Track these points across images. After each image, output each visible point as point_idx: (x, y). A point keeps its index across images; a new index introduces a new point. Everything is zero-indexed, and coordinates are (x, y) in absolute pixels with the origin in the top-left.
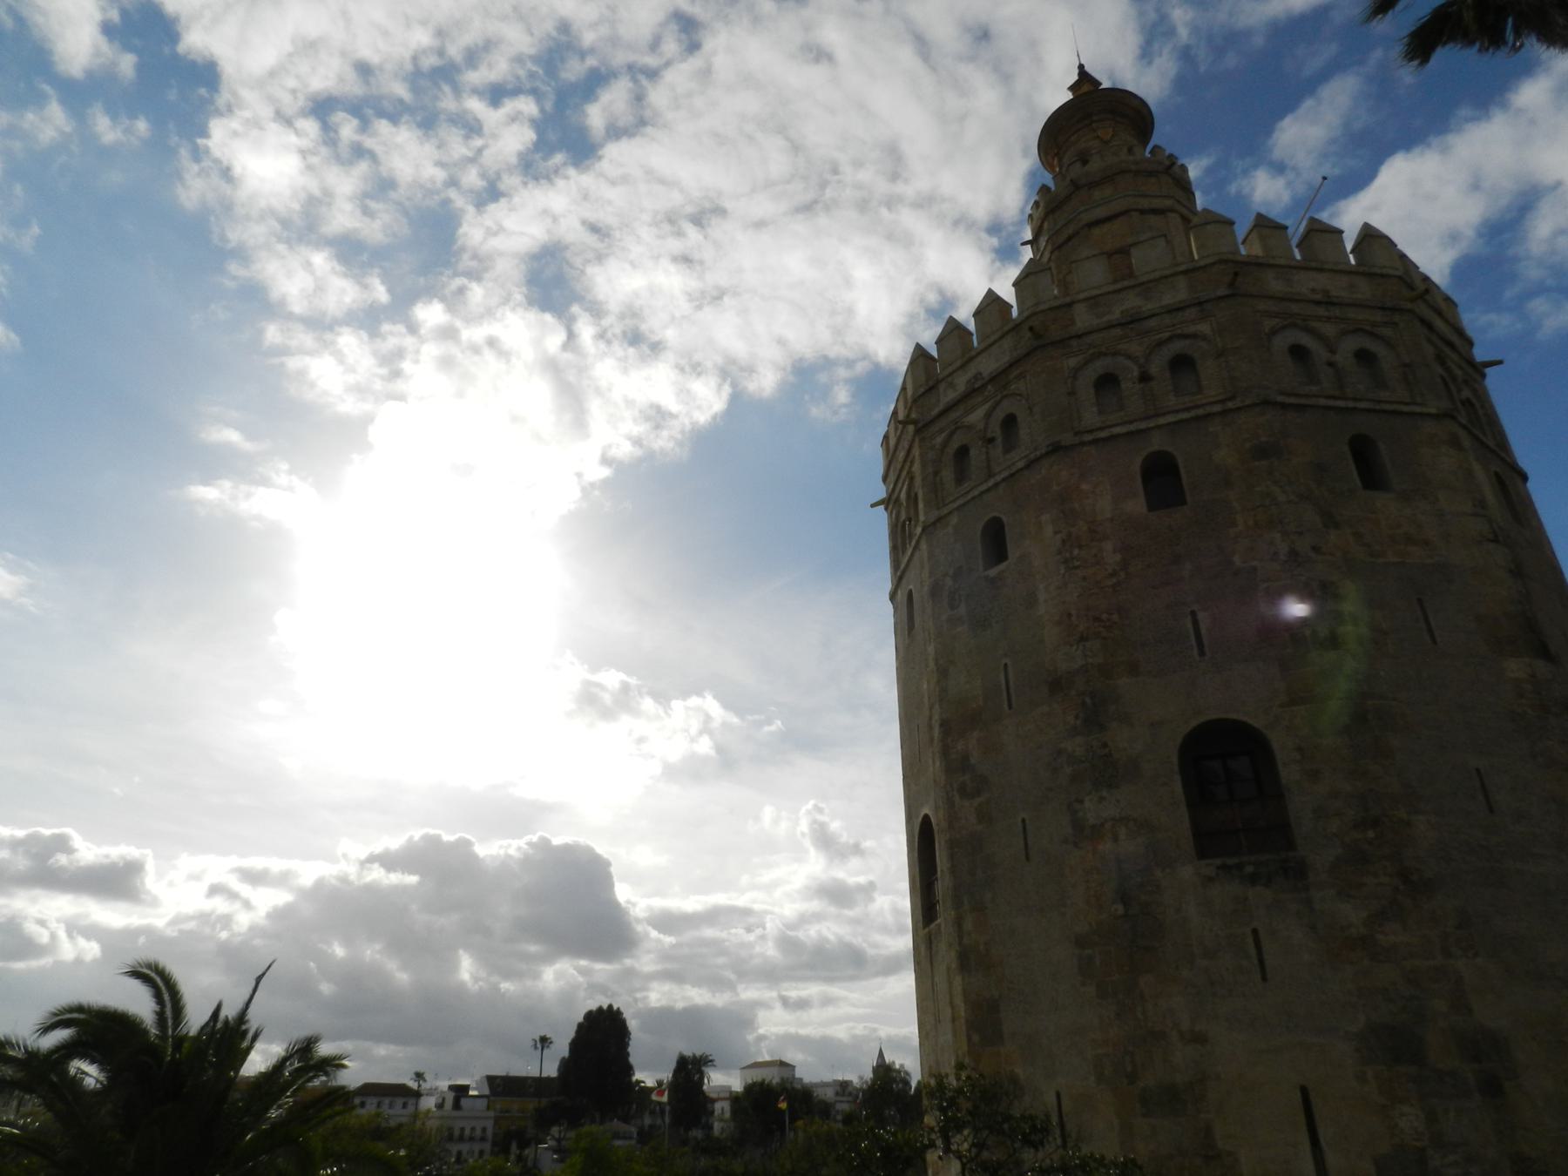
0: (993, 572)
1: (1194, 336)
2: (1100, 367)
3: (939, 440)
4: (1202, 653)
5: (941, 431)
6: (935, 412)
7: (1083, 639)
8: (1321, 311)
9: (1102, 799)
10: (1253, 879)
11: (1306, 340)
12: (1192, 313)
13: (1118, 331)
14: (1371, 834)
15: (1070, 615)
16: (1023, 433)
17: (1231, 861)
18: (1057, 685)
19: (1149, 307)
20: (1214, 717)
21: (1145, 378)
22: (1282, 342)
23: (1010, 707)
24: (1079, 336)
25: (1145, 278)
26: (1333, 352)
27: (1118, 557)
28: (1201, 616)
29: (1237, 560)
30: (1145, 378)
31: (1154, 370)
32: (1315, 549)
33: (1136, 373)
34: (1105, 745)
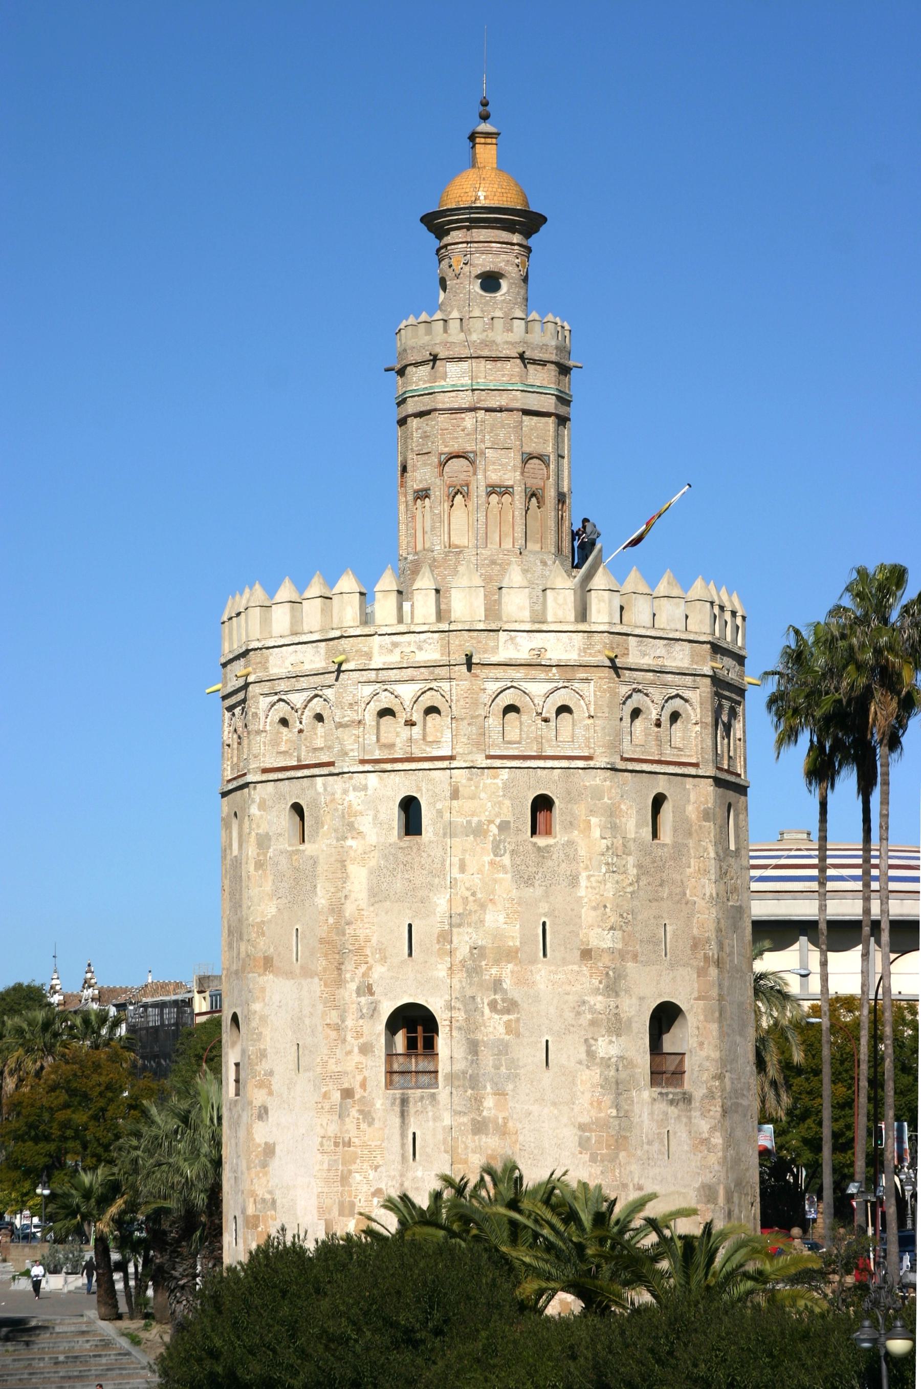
0: (541, 841)
1: (686, 701)
2: (637, 700)
5: (497, 679)
6: (495, 659)
7: (612, 928)
9: (611, 1042)
10: (672, 1102)
13: (650, 675)
15: (605, 907)
16: (580, 732)
17: (664, 1091)
18: (587, 954)
23: (545, 955)
24: (630, 669)
25: (670, 636)
28: (668, 928)
29: (688, 892)
30: (658, 725)
31: (663, 719)
34: (617, 1007)
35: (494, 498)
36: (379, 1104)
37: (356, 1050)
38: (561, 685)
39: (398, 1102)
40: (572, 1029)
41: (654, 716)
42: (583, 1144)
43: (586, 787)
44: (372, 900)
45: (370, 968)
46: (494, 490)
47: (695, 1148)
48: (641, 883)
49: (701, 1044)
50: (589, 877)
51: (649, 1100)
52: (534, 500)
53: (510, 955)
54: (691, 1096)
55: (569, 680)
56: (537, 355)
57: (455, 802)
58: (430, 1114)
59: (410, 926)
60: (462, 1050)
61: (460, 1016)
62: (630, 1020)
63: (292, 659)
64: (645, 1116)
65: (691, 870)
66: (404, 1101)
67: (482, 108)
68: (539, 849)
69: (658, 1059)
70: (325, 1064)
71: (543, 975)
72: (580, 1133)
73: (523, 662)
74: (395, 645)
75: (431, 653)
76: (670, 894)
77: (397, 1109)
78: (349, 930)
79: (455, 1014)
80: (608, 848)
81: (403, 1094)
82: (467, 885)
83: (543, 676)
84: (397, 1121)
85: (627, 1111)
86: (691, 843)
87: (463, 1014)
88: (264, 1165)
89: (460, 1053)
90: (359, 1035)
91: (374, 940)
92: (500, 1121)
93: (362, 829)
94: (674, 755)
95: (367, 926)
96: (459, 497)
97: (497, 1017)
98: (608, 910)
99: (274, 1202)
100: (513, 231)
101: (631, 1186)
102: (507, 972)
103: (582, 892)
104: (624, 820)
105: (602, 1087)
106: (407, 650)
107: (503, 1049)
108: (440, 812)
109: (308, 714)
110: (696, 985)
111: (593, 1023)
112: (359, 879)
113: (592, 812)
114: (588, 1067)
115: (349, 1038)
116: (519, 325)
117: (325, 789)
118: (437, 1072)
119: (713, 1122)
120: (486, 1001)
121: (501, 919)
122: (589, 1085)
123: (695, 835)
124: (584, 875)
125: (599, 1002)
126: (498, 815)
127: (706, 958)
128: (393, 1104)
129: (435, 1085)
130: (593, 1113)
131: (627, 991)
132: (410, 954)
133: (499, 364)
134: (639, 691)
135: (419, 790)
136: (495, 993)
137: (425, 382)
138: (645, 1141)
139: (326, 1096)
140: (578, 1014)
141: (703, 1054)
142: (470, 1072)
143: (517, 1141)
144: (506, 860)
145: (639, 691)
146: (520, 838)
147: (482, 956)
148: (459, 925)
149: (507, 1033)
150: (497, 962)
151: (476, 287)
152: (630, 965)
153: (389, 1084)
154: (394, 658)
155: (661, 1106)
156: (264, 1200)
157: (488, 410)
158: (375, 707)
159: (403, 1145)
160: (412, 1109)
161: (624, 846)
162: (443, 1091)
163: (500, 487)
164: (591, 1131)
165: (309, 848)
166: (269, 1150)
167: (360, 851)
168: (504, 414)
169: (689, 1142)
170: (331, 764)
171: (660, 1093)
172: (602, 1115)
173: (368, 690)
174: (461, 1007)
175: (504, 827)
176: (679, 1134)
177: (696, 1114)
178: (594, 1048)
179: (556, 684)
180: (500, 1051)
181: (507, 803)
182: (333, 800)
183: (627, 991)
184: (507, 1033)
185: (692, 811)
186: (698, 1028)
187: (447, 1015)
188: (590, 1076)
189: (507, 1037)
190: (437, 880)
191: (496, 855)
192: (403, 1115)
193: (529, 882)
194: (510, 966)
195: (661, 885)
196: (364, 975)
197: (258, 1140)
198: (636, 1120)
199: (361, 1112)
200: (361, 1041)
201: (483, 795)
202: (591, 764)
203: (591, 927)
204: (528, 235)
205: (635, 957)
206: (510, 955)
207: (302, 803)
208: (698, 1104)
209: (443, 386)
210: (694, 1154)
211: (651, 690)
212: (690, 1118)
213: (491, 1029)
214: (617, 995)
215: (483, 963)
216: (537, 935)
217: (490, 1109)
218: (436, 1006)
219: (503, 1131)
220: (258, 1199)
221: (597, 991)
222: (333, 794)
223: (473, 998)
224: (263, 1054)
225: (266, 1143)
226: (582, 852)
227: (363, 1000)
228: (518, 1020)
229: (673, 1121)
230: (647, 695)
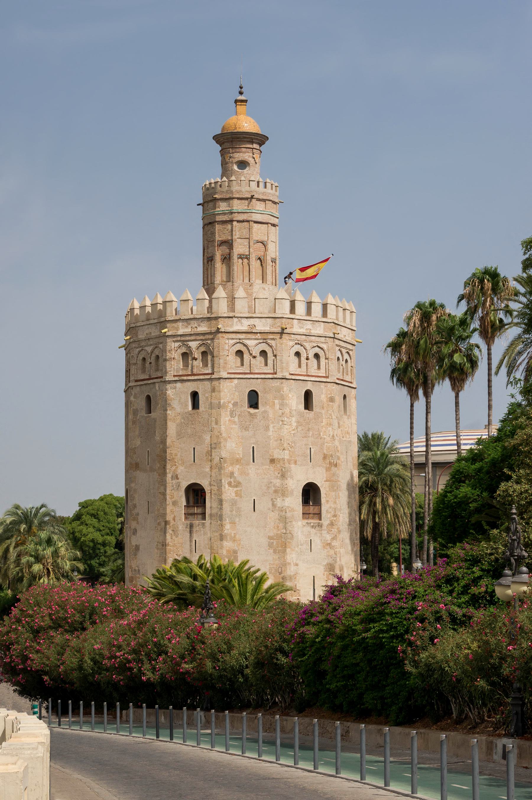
0: (252, 411)
1: (322, 349)
2: (297, 348)
3: (232, 342)
4: (311, 462)
5: (233, 339)
6: (231, 330)
7: (284, 449)
9: (283, 500)
10: (312, 527)
12: (323, 339)
14: (335, 519)
15: (281, 440)
16: (270, 362)
18: (272, 461)
19: (313, 332)
21: (307, 359)
23: (254, 461)
24: (294, 334)
27: (295, 424)
29: (321, 434)
30: (307, 359)
35: (240, 260)
36: (180, 527)
37: (171, 503)
38: (261, 341)
39: (189, 526)
40: (265, 494)
41: (305, 356)
42: (270, 545)
43: (273, 387)
44: (178, 437)
45: (177, 468)
46: (241, 257)
47: (324, 547)
49: (327, 501)
50: (274, 427)
51: (302, 526)
52: (259, 261)
53: (238, 461)
55: (265, 339)
56: (261, 197)
57: (213, 394)
58: (202, 532)
59: (194, 448)
60: (216, 504)
61: (215, 488)
62: (292, 491)
63: (147, 331)
64: (299, 533)
65: (324, 424)
66: (191, 526)
67: (240, 89)
68: (251, 414)
69: (307, 508)
70: (158, 510)
71: (252, 469)
72: (269, 540)
73: (244, 331)
74: (189, 324)
75: (203, 328)
76: (313, 434)
77: (188, 530)
78: (168, 451)
79: (213, 487)
80: (283, 414)
81: (191, 523)
82: (219, 430)
83: (253, 337)
84: (189, 534)
85: (290, 531)
86: (323, 412)
87: (216, 487)
88: (136, 555)
89: (215, 505)
90: (172, 497)
91: (179, 456)
92: (233, 535)
93: (174, 406)
95: (176, 449)
96: (225, 260)
97: (231, 488)
98: (282, 441)
99: (139, 571)
100: (252, 143)
101: (292, 564)
102: (236, 469)
103: (270, 433)
104: (290, 401)
105: (279, 520)
106: (194, 326)
107: (234, 503)
108: (207, 398)
109: (153, 355)
110: (325, 475)
111: (276, 491)
112: (172, 428)
113: (275, 398)
114: (273, 511)
115: (168, 498)
116: (254, 185)
117: (159, 389)
118: (205, 513)
119: (333, 536)
120: (227, 482)
121: (234, 445)
122: (273, 519)
123: (325, 408)
124: (271, 426)
125: (278, 482)
126: (232, 399)
127: (330, 463)
128: (186, 527)
129: (204, 518)
130: (275, 531)
131: (292, 477)
132: (194, 461)
133: (243, 201)
134: (299, 344)
135: (198, 388)
136: (231, 478)
137: (212, 209)
138: (299, 544)
139: (159, 524)
140: (268, 487)
141: (328, 506)
142: (219, 513)
143: (240, 543)
144: (236, 419)
145: (299, 344)
146: (242, 409)
147: (225, 462)
148: (215, 448)
149: (236, 496)
150: (232, 464)
151: (235, 167)
152: (293, 466)
153: (186, 518)
154: (188, 330)
156: (135, 570)
157: (238, 221)
158: (180, 351)
159: (191, 546)
160: (194, 529)
162: (208, 521)
163: (243, 255)
164: (274, 540)
165: (153, 415)
166: (137, 548)
167: (173, 415)
168: (245, 223)
170: (162, 377)
171: (307, 523)
172: (279, 532)
173: (177, 344)
174: (216, 484)
175: (235, 404)
177: (324, 532)
178: (275, 503)
179: (259, 341)
180: (233, 504)
181: (237, 393)
182: (162, 393)
183: (292, 477)
184: (236, 496)
185: (324, 398)
186: (326, 494)
187: (209, 488)
188: (273, 516)
189: (236, 498)
190: (205, 429)
191: (231, 417)
192: (191, 532)
193: (247, 429)
194: (238, 466)
195: (308, 430)
196: (174, 470)
197: (133, 544)
198: (295, 535)
199: (173, 530)
200: (173, 500)
201: (225, 390)
202: (275, 376)
203: (275, 449)
204: (260, 146)
205: (295, 463)
206: (238, 461)
207: (150, 394)
209: (218, 211)
211: (304, 344)
212: (321, 534)
213: (229, 495)
214: (287, 479)
215: (226, 465)
216: (250, 452)
217: (228, 530)
218: (205, 483)
219: (234, 540)
220: (133, 569)
221: (277, 477)
222: (162, 391)
223: (221, 480)
224: (135, 506)
225: (136, 545)
226: (271, 415)
227: (174, 481)
228: (241, 490)
230: (302, 345)
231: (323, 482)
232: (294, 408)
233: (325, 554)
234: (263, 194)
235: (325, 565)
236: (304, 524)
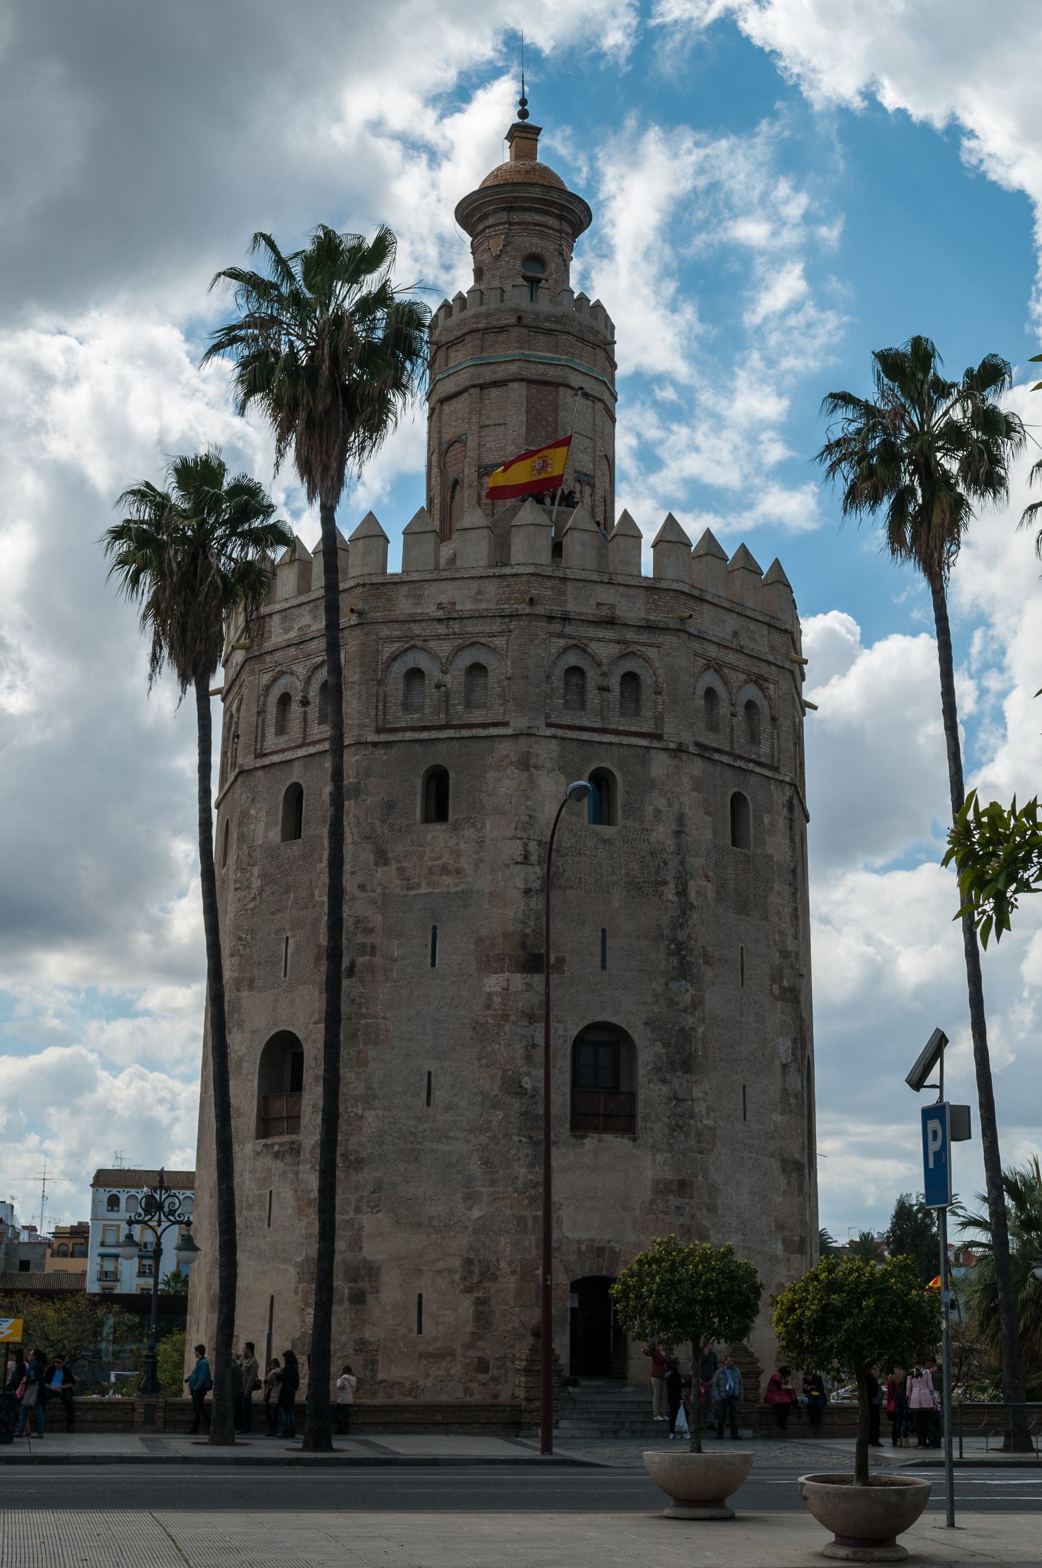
4: (285, 976)
8: (442, 629)
10: (277, 1155)
11: (423, 662)
13: (292, 651)
20: (281, 1029)
21: (305, 703)
22: (399, 668)
26: (445, 672)
28: (291, 941)
29: (316, 893)
30: (305, 703)
32: (362, 887)
33: (299, 698)
48: (264, 896)
51: (252, 1154)
54: (300, 1146)
64: (247, 1175)
94: (321, 733)
104: (252, 827)
131: (240, 1026)
152: (245, 993)
155: (265, 1161)
161: (250, 855)
169: (293, 1204)
171: (266, 1145)
176: (283, 1194)
205: (251, 986)
208: (308, 1155)
210: (300, 1220)
211: (294, 668)
212: (297, 1173)
229: (277, 1179)
231: (312, 1026)
232: (259, 842)
233: (304, 1232)
234: (459, 325)
235: (301, 1265)
236: (258, 1148)
